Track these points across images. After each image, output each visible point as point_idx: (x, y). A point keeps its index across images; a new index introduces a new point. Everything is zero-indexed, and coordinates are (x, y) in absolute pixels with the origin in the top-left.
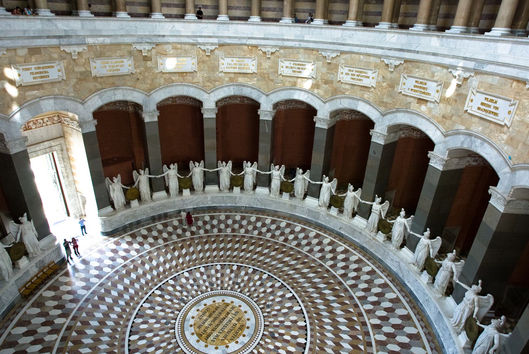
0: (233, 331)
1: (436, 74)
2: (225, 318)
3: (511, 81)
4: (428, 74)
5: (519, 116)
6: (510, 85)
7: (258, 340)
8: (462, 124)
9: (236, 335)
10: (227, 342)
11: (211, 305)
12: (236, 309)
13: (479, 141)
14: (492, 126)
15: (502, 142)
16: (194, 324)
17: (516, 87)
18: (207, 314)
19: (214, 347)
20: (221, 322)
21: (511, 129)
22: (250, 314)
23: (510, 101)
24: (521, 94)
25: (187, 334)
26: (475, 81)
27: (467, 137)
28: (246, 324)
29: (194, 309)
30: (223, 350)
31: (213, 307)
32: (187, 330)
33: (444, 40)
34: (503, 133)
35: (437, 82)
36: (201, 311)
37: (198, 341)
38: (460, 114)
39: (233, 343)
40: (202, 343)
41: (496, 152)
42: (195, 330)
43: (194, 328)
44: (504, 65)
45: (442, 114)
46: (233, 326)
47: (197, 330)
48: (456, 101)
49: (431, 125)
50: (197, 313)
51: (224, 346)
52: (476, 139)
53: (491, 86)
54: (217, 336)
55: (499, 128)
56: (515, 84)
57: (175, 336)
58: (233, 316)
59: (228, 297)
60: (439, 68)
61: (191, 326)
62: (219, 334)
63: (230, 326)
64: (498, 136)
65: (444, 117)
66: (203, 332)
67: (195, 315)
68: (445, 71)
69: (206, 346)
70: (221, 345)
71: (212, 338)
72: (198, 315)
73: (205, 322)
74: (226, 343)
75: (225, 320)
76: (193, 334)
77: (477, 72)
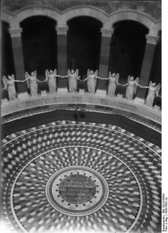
0: (79, 179)
2: (73, 188)
7: (77, 166)
9: (80, 177)
10: (88, 179)
11: (67, 201)
12: (61, 186)
16: (88, 201)
18: (76, 199)
19: (95, 182)
20: (77, 188)
22: (61, 177)
25: (97, 200)
28: (70, 176)
29: (77, 209)
30: (94, 178)
31: (68, 199)
32: (96, 202)
36: (76, 203)
37: (98, 192)
39: (86, 175)
40: (97, 189)
42: (92, 198)
43: (91, 199)
46: (75, 181)
47: (91, 197)
50: (79, 205)
51: (91, 178)
54: (87, 185)
57: (104, 205)
58: (68, 184)
59: (53, 195)
61: (91, 202)
62: (86, 185)
63: (77, 182)
66: (90, 193)
67: (82, 205)
69: (97, 186)
70: (92, 180)
71: (90, 187)
72: (80, 203)
73: (82, 197)
74: (89, 178)
75: (74, 187)
76: (95, 197)
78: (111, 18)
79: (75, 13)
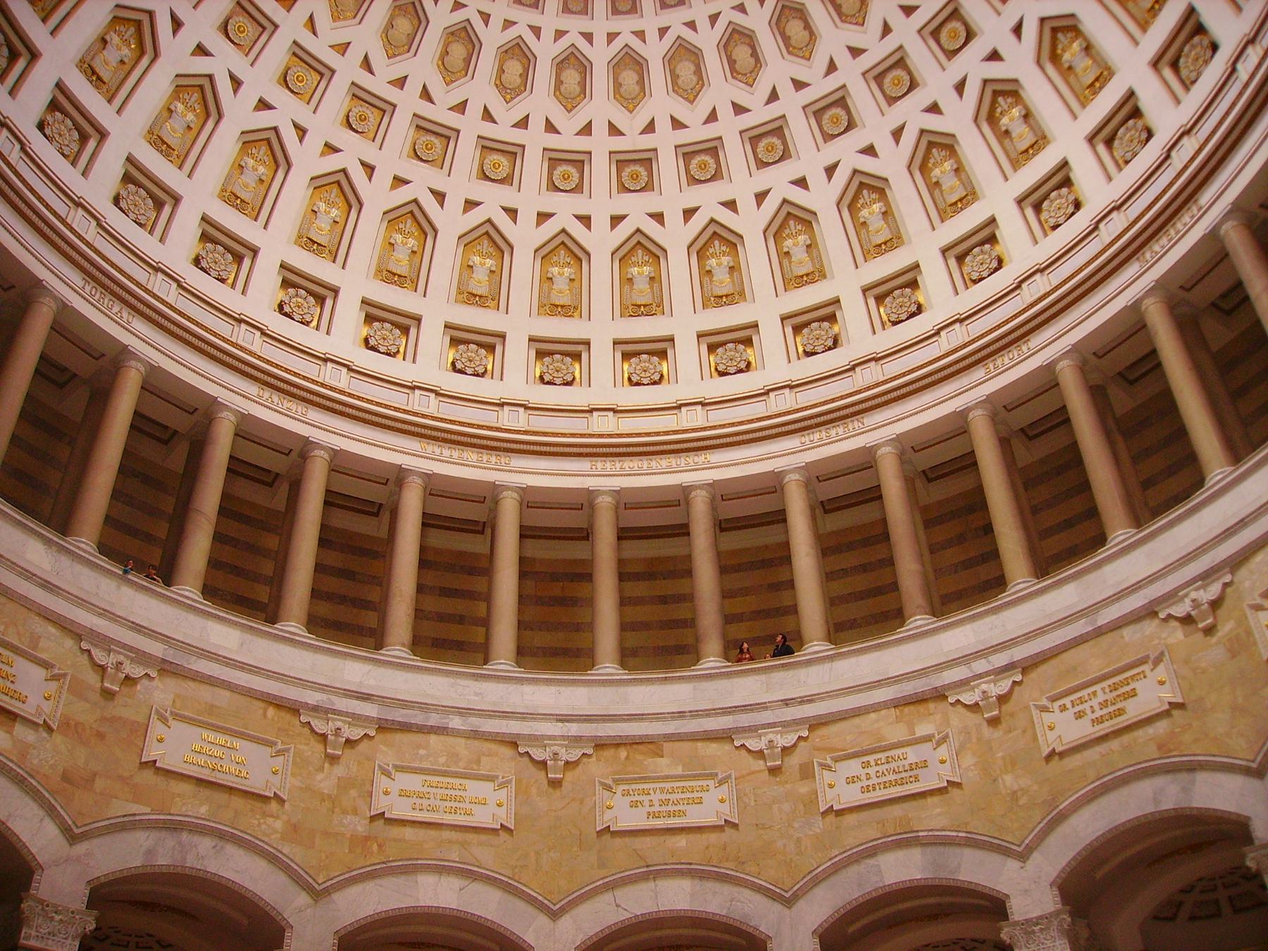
1: (43, 644)
3: (261, 705)
4: (18, 633)
5: (299, 778)
6: (261, 712)
8: (136, 800)
13: (206, 844)
14: (238, 802)
15: (273, 837)
17: (276, 718)
21: (287, 805)
23: (270, 744)
24: (291, 733)
26: (162, 692)
27: (164, 834)
33: (65, 561)
34: (272, 816)
35: (46, 665)
38: (126, 774)
41: (262, 864)
44: (243, 668)
45: (60, 769)
48: (101, 736)
49: (28, 800)
52: (196, 839)
53: (211, 709)
55: (259, 805)
56: (271, 712)
60: (52, 629)
64: (259, 825)
65: (66, 777)
68: (69, 643)
77: (167, 669)
78: (801, 904)
79: (618, 906)
